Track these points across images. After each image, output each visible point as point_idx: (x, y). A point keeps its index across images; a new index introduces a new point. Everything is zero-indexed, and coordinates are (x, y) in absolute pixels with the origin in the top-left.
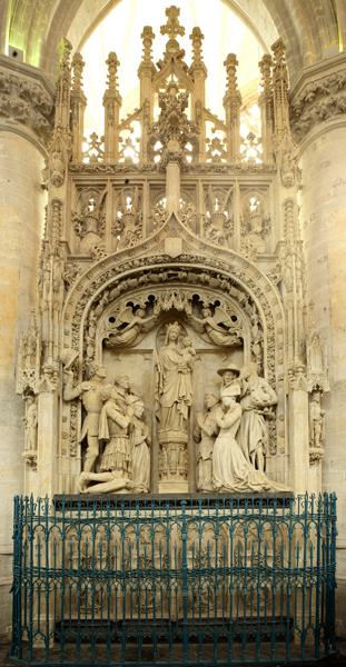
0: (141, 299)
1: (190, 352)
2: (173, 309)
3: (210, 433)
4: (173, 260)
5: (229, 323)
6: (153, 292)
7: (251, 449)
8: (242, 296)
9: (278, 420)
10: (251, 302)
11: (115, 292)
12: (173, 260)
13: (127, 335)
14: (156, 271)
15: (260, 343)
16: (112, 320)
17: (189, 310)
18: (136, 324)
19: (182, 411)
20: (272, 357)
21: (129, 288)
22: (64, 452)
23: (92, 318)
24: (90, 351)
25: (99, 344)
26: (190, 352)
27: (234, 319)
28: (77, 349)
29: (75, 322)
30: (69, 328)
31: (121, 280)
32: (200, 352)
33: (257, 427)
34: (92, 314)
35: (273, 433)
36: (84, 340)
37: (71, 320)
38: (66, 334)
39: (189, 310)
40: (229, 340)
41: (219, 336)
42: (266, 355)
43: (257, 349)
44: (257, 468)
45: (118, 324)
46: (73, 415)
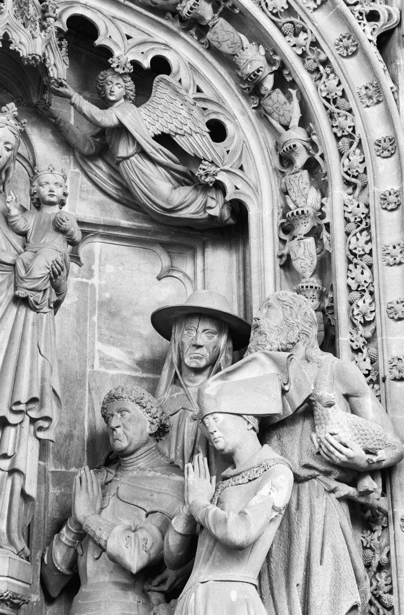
1: (59, 229)
3: (135, 561)
5: (197, 142)
8: (253, 58)
10: (284, 81)
15: (315, 233)
17: (59, 68)
26: (59, 229)
27: (217, 131)
32: (89, 229)
35: (382, 578)
39: (59, 68)
40: (191, 205)
41: (158, 185)
42: (341, 280)
43: (305, 254)
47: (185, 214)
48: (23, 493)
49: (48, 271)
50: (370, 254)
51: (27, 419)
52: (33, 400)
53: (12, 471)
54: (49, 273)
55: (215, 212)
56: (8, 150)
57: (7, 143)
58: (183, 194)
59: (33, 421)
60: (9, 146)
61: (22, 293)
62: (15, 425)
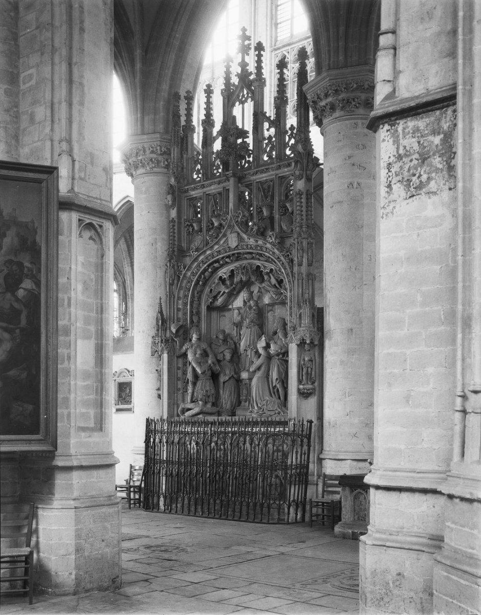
0: (223, 272)
2: (241, 281)
4: (234, 249)
6: (232, 267)
7: (274, 385)
11: (207, 274)
12: (234, 249)
13: (220, 301)
14: (228, 257)
18: (224, 292)
21: (216, 270)
22: (178, 390)
23: (196, 295)
24: (195, 319)
25: (204, 308)
31: (209, 266)
45: (214, 294)
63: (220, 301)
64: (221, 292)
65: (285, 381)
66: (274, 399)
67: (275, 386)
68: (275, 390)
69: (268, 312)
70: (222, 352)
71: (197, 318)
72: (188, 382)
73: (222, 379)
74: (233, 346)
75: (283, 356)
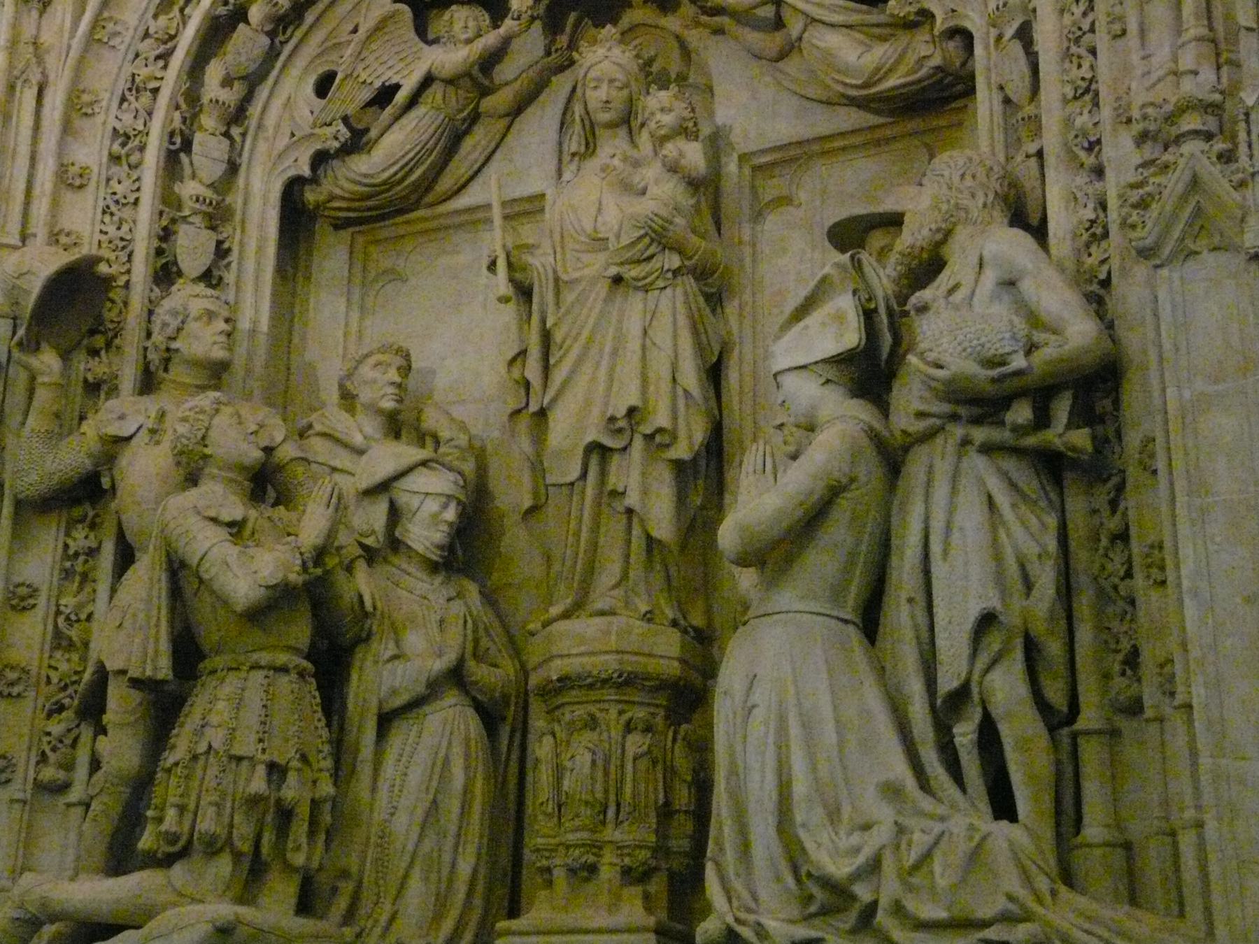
7: (947, 683)
9: (1133, 472)
16: (324, 86)
18: (428, 81)
19: (632, 499)
20: (1087, 92)
24: (193, 248)
28: (126, 245)
29: (128, 121)
30: (90, 152)
33: (972, 537)
34: (214, 72)
36: (169, 199)
37: (108, 117)
38: (70, 180)
44: (1004, 807)
45: (348, 98)
46: (75, 570)
47: (892, 82)
48: (650, 540)
49: (642, 232)
50: (1092, 30)
51: (638, 443)
52: (632, 411)
53: (630, 511)
54: (646, 234)
55: (937, 61)
56: (621, 89)
57: (611, 81)
58: (879, 53)
59: (649, 438)
60: (617, 84)
61: (613, 270)
62: (625, 449)
63: (397, 143)
64: (397, 87)
65: (1054, 648)
66: (967, 816)
67: (960, 696)
68: (965, 733)
69: (758, 216)
70: (383, 487)
71: (207, 240)
72: (93, 709)
73: (376, 679)
74: (469, 467)
75: (1042, 420)
